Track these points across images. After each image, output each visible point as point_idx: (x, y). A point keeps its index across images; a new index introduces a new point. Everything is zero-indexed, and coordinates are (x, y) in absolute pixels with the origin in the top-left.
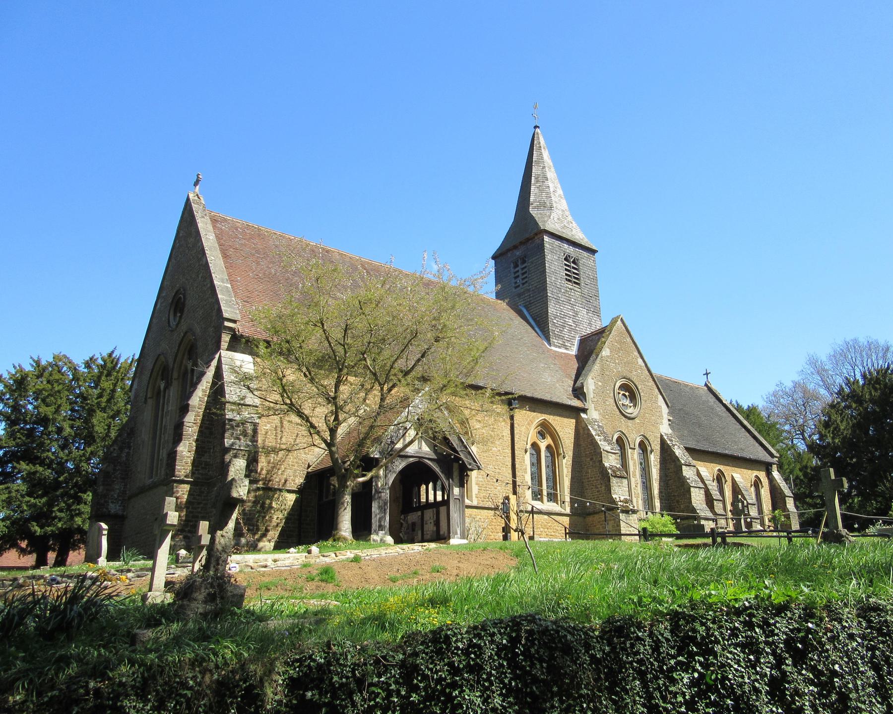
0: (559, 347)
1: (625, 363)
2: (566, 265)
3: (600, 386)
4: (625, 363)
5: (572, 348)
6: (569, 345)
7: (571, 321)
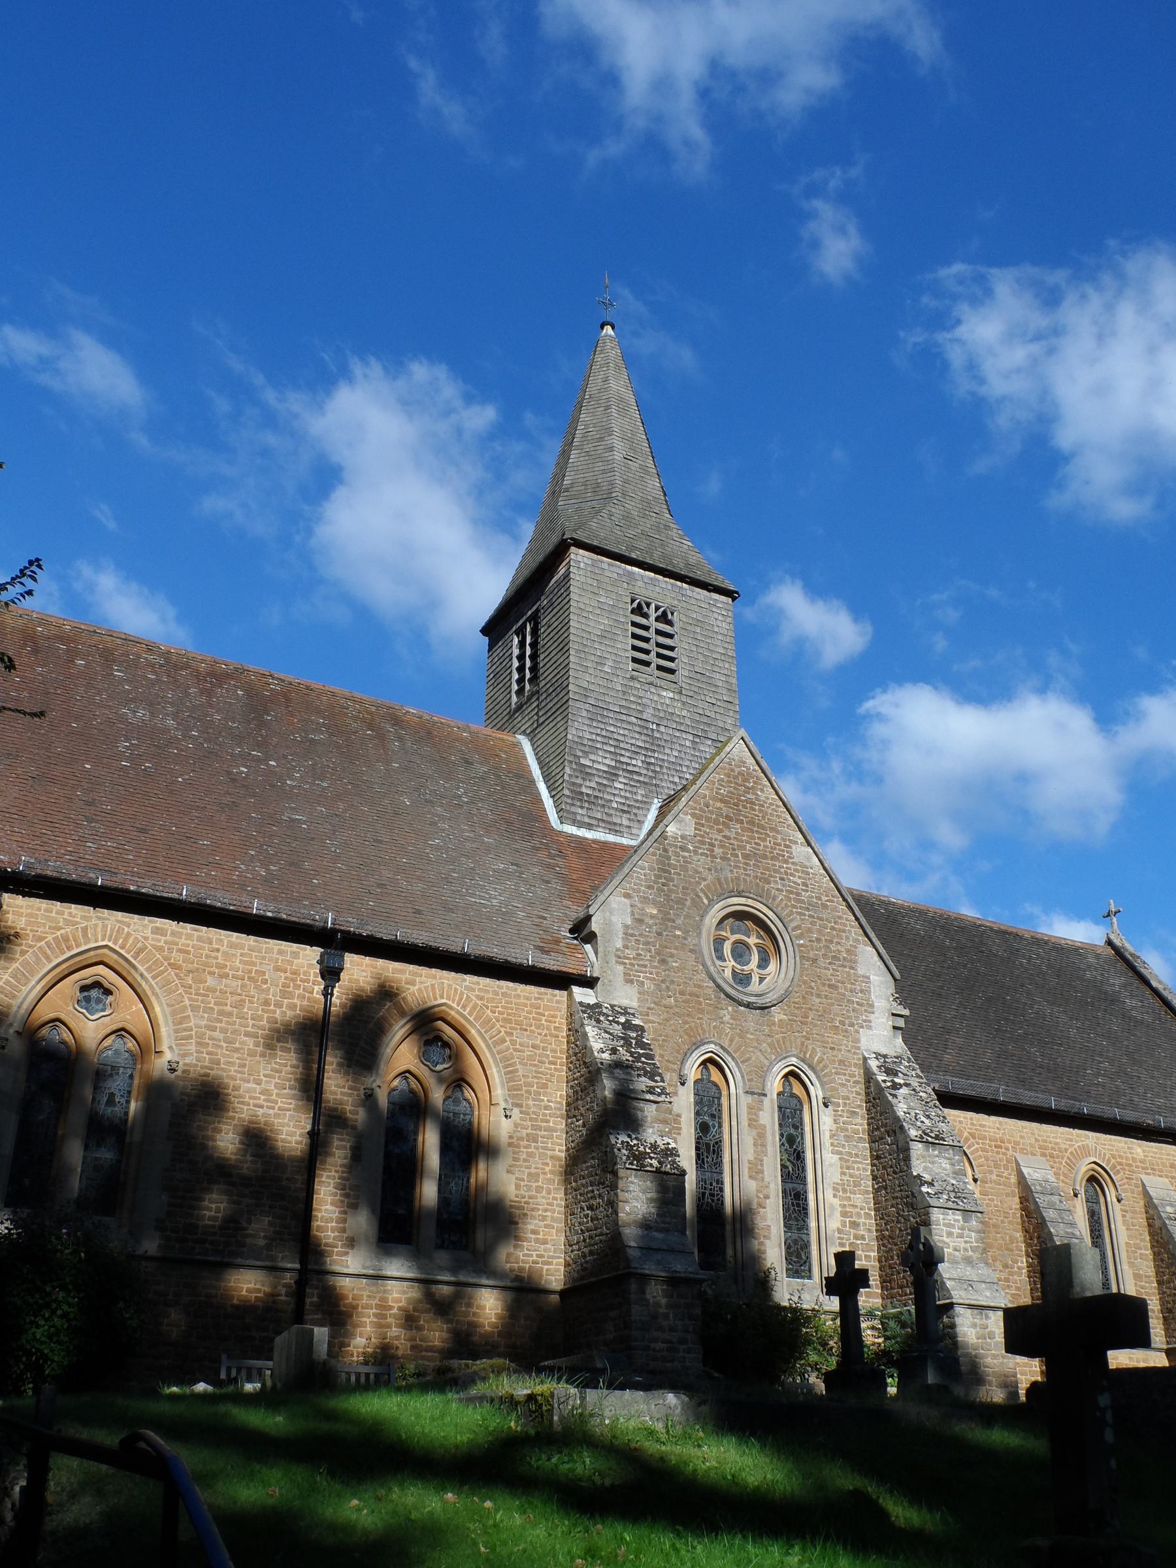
0: (589, 827)
1: (746, 856)
2: (634, 624)
3: (652, 917)
4: (746, 856)
5: (634, 831)
6: (625, 822)
7: (640, 764)
